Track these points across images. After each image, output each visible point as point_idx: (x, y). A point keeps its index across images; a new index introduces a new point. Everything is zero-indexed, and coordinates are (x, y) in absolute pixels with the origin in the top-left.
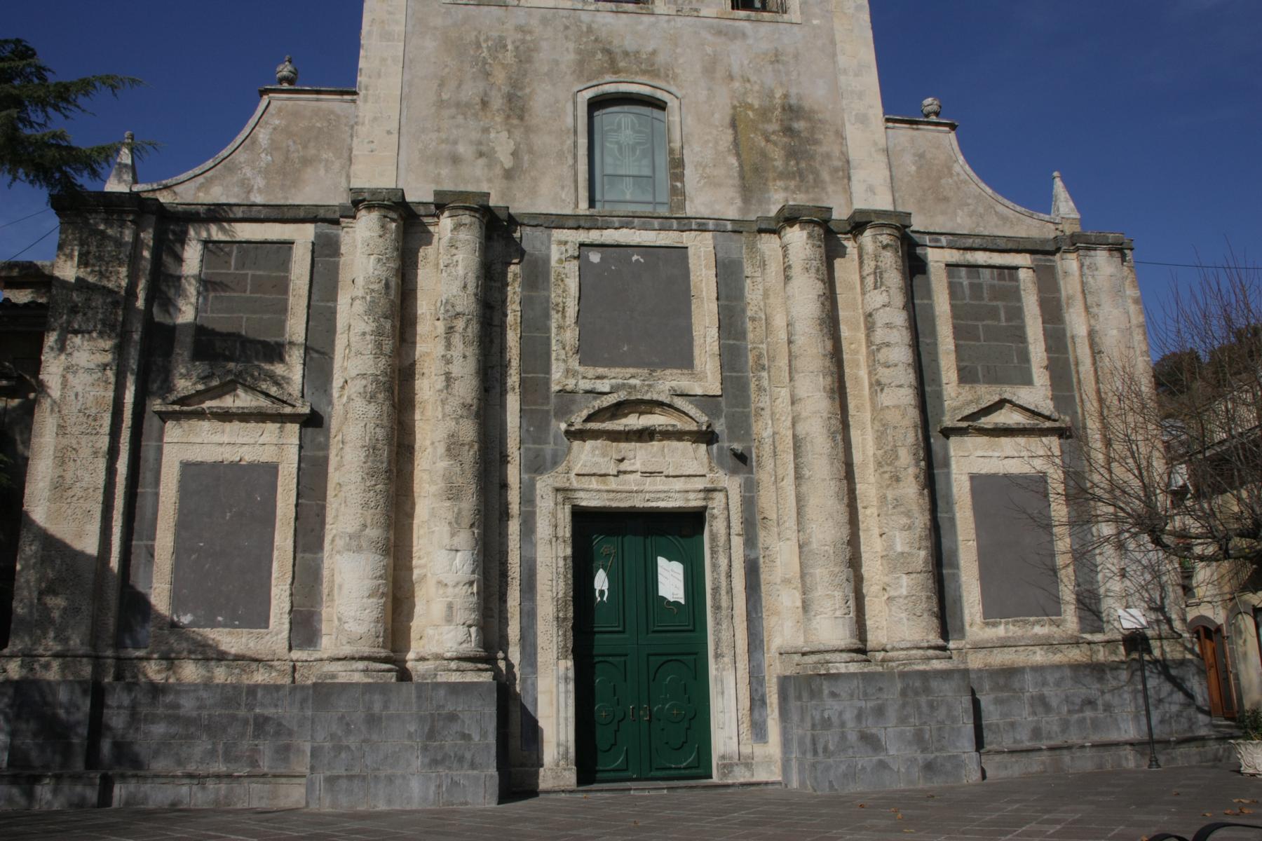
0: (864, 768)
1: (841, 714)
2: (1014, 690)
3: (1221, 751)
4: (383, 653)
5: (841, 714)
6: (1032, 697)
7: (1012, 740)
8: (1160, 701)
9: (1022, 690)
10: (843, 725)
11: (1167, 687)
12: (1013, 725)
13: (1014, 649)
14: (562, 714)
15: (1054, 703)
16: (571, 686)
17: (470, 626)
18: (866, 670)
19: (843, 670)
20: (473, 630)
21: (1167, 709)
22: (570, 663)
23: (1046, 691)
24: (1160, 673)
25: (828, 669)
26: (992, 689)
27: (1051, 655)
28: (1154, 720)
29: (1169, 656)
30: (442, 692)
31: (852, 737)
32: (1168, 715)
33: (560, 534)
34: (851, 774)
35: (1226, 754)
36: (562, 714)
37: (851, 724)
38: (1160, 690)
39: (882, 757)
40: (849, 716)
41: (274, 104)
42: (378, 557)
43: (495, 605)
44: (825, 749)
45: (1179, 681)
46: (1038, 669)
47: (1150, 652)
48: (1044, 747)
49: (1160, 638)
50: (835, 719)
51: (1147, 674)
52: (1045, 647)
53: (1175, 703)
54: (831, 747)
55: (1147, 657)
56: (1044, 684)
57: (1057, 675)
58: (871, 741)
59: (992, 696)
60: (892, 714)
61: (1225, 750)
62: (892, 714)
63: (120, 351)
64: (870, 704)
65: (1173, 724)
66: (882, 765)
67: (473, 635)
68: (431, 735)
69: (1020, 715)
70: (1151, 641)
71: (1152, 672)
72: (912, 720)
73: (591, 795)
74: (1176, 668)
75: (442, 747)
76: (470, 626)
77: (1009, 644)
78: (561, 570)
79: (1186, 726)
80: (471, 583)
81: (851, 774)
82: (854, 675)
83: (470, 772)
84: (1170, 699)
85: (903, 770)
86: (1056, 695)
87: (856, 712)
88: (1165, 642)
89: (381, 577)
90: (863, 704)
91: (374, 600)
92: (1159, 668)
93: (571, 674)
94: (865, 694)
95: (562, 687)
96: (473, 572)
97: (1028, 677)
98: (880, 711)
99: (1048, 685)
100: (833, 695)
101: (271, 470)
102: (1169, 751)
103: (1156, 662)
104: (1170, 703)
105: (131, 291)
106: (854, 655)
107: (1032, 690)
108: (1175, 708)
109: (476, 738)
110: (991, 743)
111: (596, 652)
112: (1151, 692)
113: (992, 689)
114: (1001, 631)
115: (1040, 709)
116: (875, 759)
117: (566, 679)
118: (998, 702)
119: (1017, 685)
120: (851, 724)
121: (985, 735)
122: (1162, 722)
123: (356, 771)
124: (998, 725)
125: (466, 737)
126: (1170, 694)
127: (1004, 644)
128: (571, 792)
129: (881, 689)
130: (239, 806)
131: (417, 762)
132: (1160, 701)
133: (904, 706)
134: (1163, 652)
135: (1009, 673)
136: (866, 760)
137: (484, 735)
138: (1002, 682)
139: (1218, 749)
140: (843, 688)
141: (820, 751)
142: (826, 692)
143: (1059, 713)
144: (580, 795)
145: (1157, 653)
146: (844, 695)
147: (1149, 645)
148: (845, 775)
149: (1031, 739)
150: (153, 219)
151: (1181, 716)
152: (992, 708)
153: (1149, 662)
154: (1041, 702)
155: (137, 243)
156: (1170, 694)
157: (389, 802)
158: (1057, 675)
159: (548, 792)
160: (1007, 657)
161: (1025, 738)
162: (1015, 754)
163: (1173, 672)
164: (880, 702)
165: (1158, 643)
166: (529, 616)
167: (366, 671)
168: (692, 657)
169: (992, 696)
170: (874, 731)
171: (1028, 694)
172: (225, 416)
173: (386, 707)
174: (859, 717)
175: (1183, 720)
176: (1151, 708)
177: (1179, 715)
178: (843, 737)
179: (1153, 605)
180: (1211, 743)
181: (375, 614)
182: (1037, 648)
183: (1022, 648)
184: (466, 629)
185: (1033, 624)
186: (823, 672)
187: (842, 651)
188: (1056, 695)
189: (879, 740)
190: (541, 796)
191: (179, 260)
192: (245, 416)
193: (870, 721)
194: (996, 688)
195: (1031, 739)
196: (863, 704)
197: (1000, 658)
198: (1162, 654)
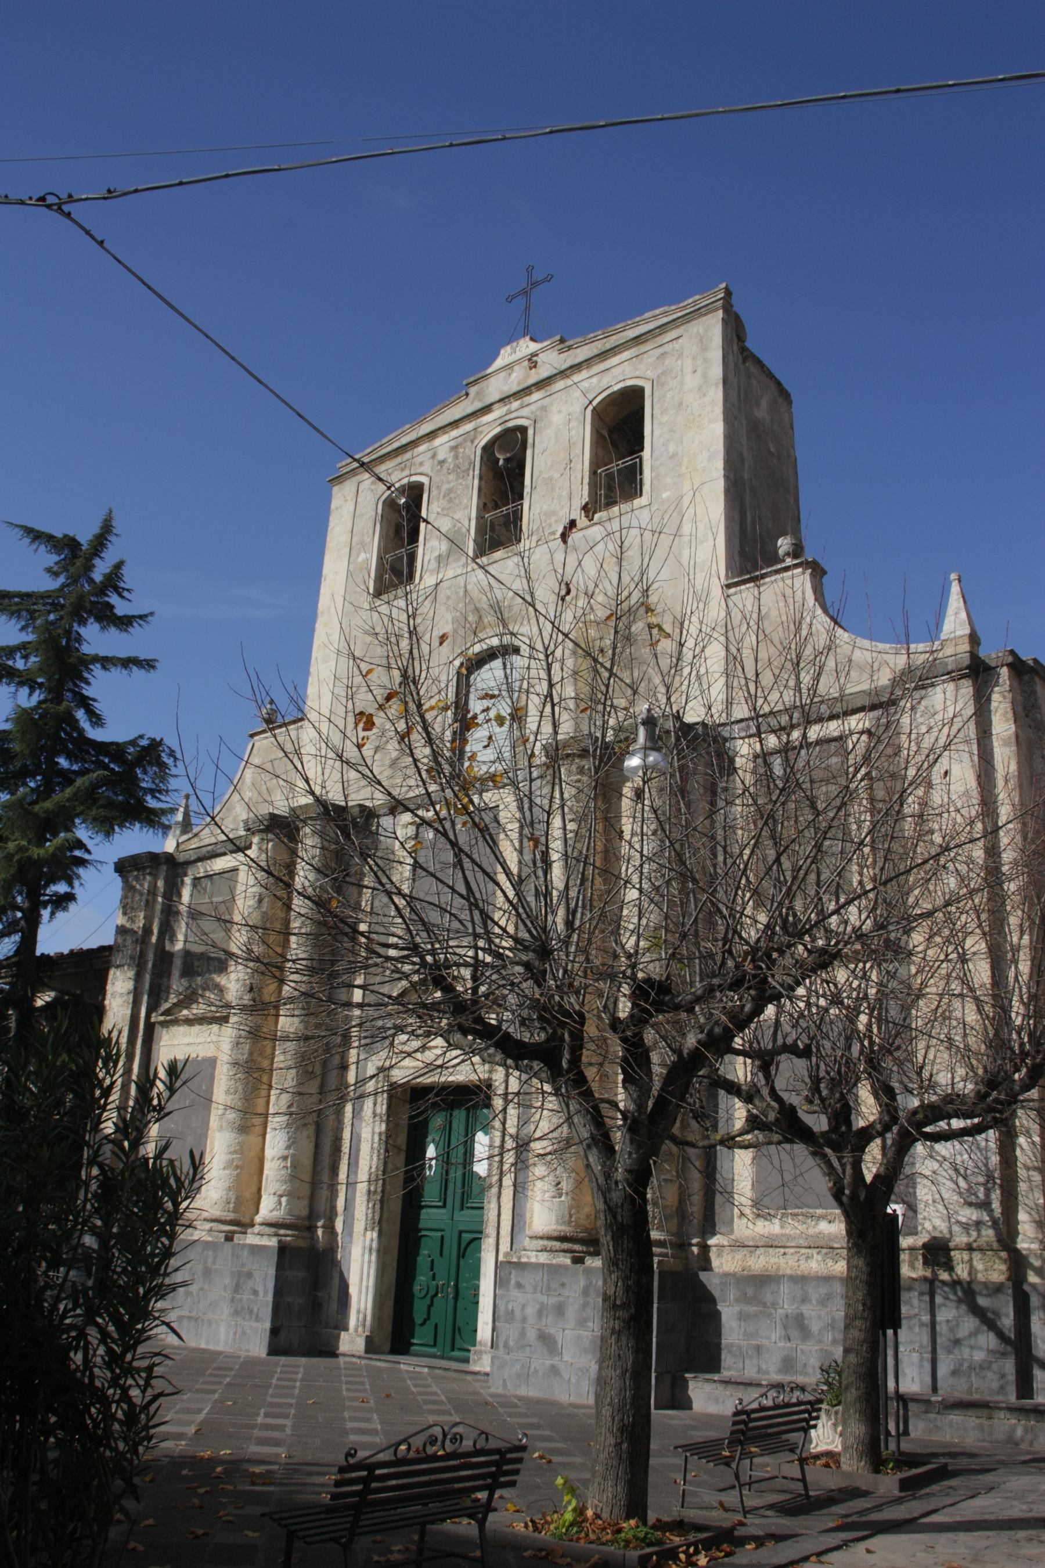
0: (536, 1371)
1: (524, 1306)
2: (765, 1305)
3: (1019, 1432)
4: (231, 1216)
5: (524, 1306)
6: (787, 1316)
7: (755, 1369)
8: (957, 1342)
9: (774, 1305)
10: (524, 1320)
11: (969, 1323)
12: (758, 1349)
13: (782, 1250)
14: (364, 1283)
15: (815, 1327)
16: (374, 1257)
17: (281, 1196)
18: (554, 1262)
19: (533, 1260)
20: (284, 1200)
21: (966, 1356)
22: (375, 1235)
23: (807, 1310)
24: (960, 1301)
25: (519, 1258)
26: (737, 1300)
27: (830, 1263)
28: (942, 1371)
29: (980, 1277)
30: (246, 1252)
31: (532, 1334)
32: (966, 1365)
33: (378, 1111)
34: (525, 1376)
35: (1029, 1437)
36: (364, 1283)
37: (531, 1320)
38: (958, 1325)
39: (555, 1361)
40: (531, 1311)
41: (257, 745)
42: (233, 1135)
43: (325, 1177)
44: (506, 1345)
45: (990, 1315)
46: (801, 1280)
47: (950, 1268)
48: (764, 1383)
49: (970, 1248)
50: (518, 1314)
51: (938, 1300)
52: (824, 1251)
53: (981, 1348)
54: (511, 1343)
55: (944, 1276)
56: (804, 1300)
57: (823, 1290)
58: (547, 1341)
59: (736, 1309)
60: (572, 1312)
61: (1026, 1430)
62: (572, 1312)
63: (138, 978)
64: (553, 1300)
65: (973, 1377)
66: (554, 1371)
67: (284, 1204)
68: (237, 1288)
69: (768, 1338)
70: (952, 1253)
71: (947, 1298)
72: (591, 1324)
73: (373, 1363)
74: (989, 1295)
75: (241, 1300)
76: (281, 1196)
77: (776, 1243)
78: (376, 1145)
79: (995, 1385)
80: (285, 1158)
81: (525, 1376)
82: (541, 1266)
83: (255, 1324)
84: (972, 1342)
85: (573, 1380)
86: (819, 1317)
87: (537, 1307)
88: (977, 1256)
89: (235, 1152)
90: (544, 1299)
91: (227, 1172)
92: (960, 1294)
93: (375, 1245)
94: (549, 1288)
95: (367, 1256)
96: (288, 1148)
97: (785, 1288)
98: (560, 1310)
99: (810, 1301)
100: (519, 1285)
101: (212, 1062)
102: (932, 1416)
103: (956, 1283)
104: (972, 1348)
105: (147, 930)
106: (545, 1242)
107: (788, 1307)
108: (979, 1356)
109: (261, 1294)
110: (729, 1369)
111: (421, 1225)
112: (942, 1329)
113: (737, 1300)
114: (774, 1228)
115: (795, 1333)
116: (548, 1362)
117: (371, 1249)
118: (742, 1317)
119: (769, 1298)
120: (531, 1320)
121: (723, 1357)
122: (954, 1373)
123: (193, 1314)
124: (740, 1347)
125: (255, 1293)
126: (974, 1334)
127: (771, 1244)
128: (359, 1357)
129: (563, 1285)
130: (477, 1369)
131: (225, 1310)
132: (957, 1342)
133: (585, 1306)
134: (972, 1270)
135: (764, 1280)
136: (541, 1362)
137: (266, 1293)
138: (750, 1291)
139: (1013, 1429)
140: (529, 1279)
141: (501, 1345)
142: (513, 1282)
143: (820, 1342)
144: (364, 1362)
145: (962, 1272)
146: (529, 1288)
147: (950, 1259)
148: (519, 1376)
149: (780, 1371)
150: (164, 868)
151: (989, 1368)
152: (734, 1324)
153: (944, 1283)
154: (799, 1324)
155: (153, 891)
156: (974, 1334)
157: (207, 1342)
158: (823, 1290)
159: (344, 1355)
160: (773, 1260)
161: (773, 1368)
162: (729, 1386)
163: (982, 1301)
164: (561, 1299)
165: (966, 1256)
166: (351, 1185)
167: (211, 1230)
168: (439, 1234)
169: (736, 1309)
170: (552, 1331)
171: (780, 1311)
172: (189, 1022)
173: (214, 1262)
174: (540, 1313)
175: (990, 1374)
176: (939, 1351)
177: (984, 1366)
178: (523, 1333)
179: (973, 1199)
180: (1002, 1414)
181: (227, 1184)
182: (815, 1251)
183: (792, 1250)
184: (276, 1198)
185: (820, 1217)
186: (515, 1260)
187: (542, 1238)
188: (819, 1317)
189: (556, 1343)
190: (341, 1359)
191: (180, 896)
192: (201, 1020)
193: (550, 1320)
194: (743, 1299)
195: (780, 1371)
196: (544, 1299)
197: (760, 1262)
198: (970, 1274)
